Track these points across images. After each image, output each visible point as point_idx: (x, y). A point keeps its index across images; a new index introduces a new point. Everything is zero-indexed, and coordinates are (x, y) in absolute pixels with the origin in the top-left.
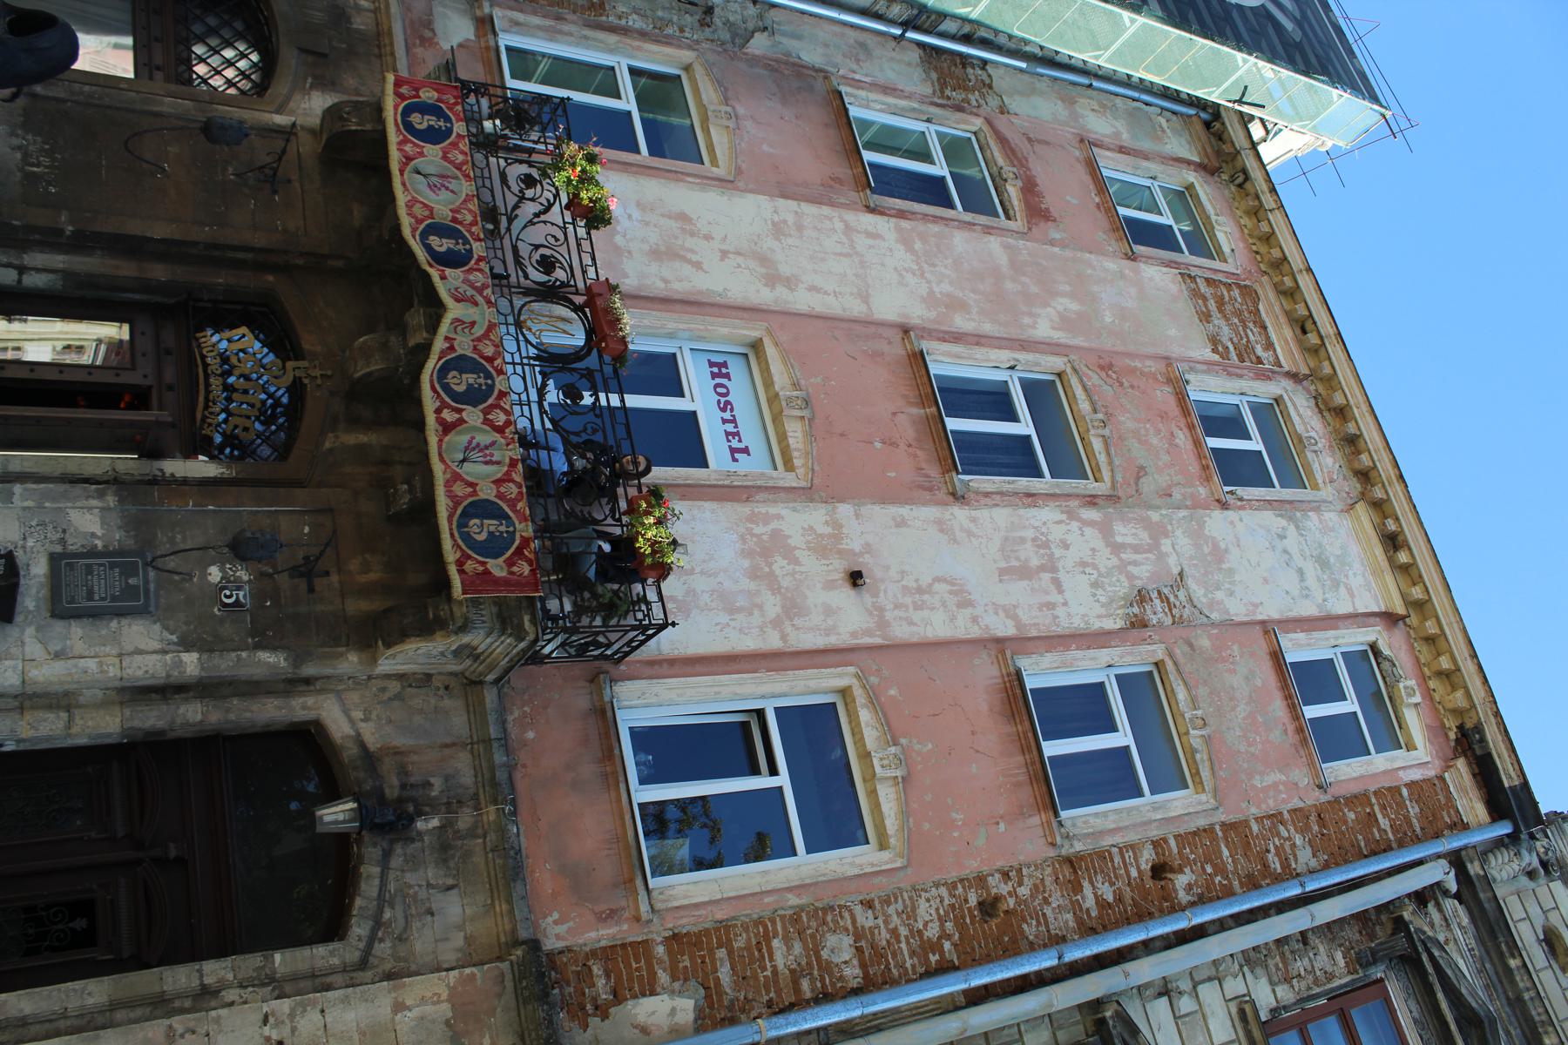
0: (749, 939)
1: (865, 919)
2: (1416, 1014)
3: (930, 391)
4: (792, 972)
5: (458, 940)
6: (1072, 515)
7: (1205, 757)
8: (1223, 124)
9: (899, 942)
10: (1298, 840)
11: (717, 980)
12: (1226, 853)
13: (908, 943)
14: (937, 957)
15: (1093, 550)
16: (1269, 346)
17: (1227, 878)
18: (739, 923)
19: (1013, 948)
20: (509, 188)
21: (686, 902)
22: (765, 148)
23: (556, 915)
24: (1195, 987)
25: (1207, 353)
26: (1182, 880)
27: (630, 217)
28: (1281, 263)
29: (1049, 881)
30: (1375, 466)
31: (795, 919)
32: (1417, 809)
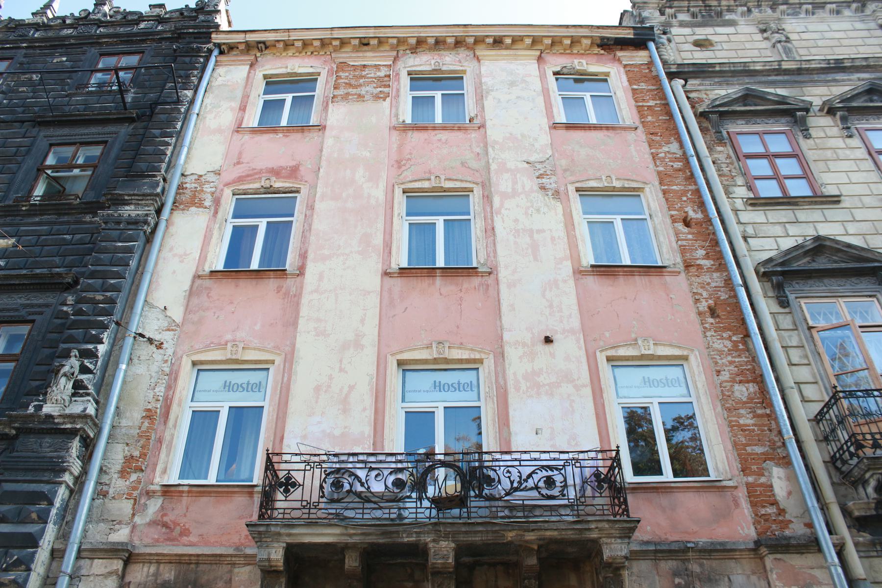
0: (741, 435)
1: (725, 376)
2: (744, 122)
3: (426, 271)
4: (754, 417)
5: (754, 578)
6: (498, 213)
7: (626, 182)
8: (224, 44)
9: (734, 362)
10: (666, 149)
11: (762, 454)
12: (675, 187)
13: (734, 357)
14: (740, 345)
15: (518, 206)
16: (377, 67)
17: (688, 191)
18: (733, 438)
19: (737, 306)
20: (343, 499)
21: (726, 463)
22: (257, 327)
23: (739, 528)
24: (741, 223)
25: (387, 104)
26: (691, 214)
27: (319, 423)
28: (324, 43)
29: (698, 280)
30: (456, 37)
31: (729, 410)
32: (643, 84)
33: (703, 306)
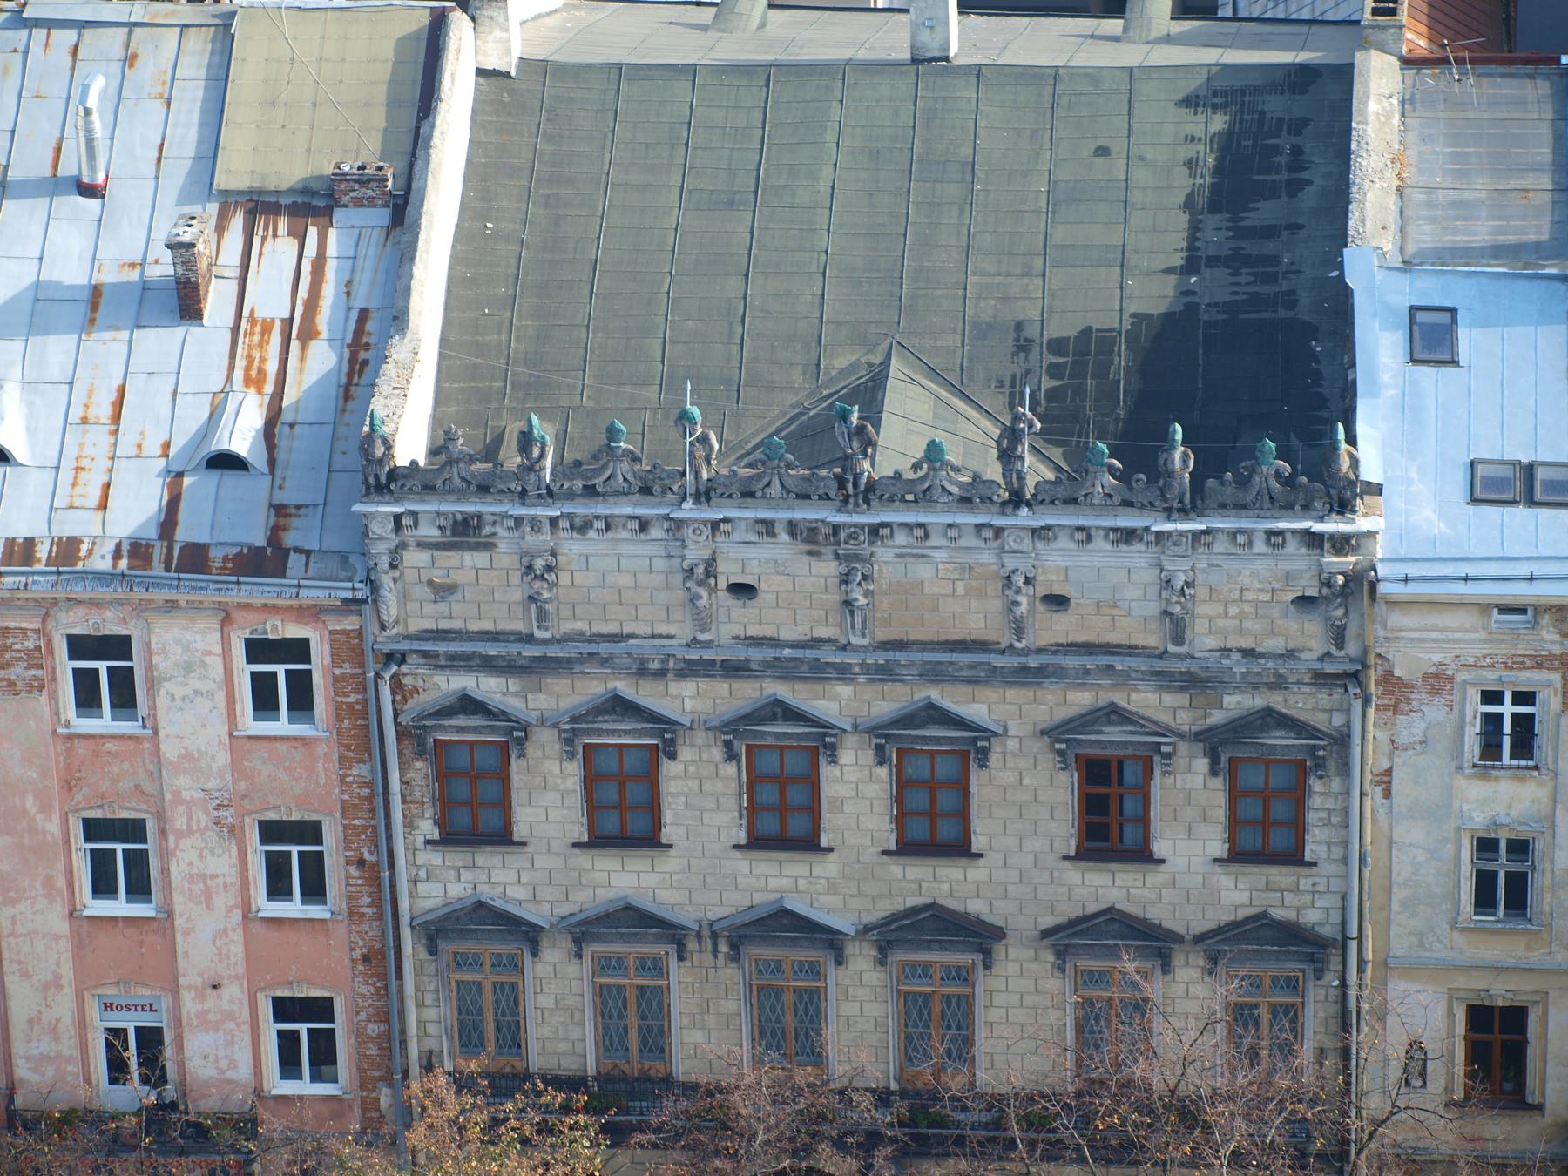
1: (363, 1016)
33: (357, 954)
